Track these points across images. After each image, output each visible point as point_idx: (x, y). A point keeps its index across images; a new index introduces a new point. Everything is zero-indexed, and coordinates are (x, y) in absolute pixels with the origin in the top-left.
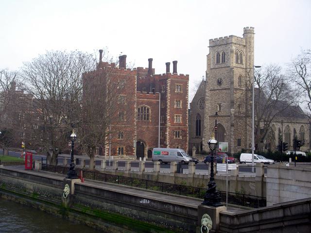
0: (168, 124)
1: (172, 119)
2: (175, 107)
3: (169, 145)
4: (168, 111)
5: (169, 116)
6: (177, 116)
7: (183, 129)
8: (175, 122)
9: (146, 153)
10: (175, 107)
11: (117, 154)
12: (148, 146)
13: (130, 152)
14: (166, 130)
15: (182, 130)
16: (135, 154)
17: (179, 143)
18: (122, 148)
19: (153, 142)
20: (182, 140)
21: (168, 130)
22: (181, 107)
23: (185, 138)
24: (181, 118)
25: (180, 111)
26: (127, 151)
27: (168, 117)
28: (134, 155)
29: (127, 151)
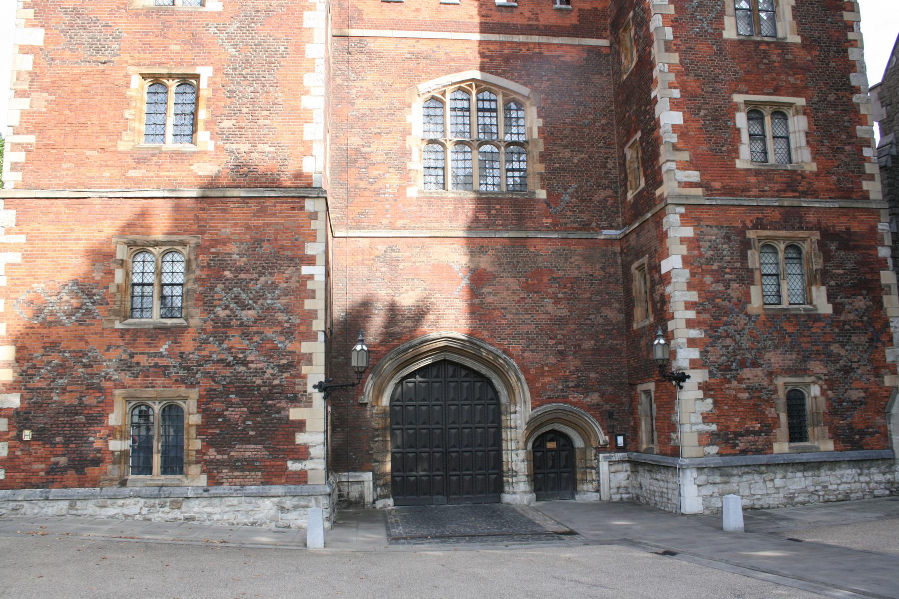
0: (678, 177)
1: (711, 137)
2: (729, 33)
3: (698, 376)
4: (665, 63)
5: (675, 105)
6: (755, 113)
7: (840, 224)
8: (745, 159)
9: (516, 458)
10: (729, 33)
11: (114, 471)
12: (524, 392)
13: (250, 451)
14: (663, 236)
15: (827, 235)
16: (316, 466)
17: (806, 359)
18: (173, 413)
19: (573, 363)
20: (832, 320)
21: (677, 229)
22: (797, 39)
23: (860, 303)
24: (798, 124)
25: (791, 67)
26: (209, 443)
27: (670, 118)
28: (301, 478)
29: (218, 433)
